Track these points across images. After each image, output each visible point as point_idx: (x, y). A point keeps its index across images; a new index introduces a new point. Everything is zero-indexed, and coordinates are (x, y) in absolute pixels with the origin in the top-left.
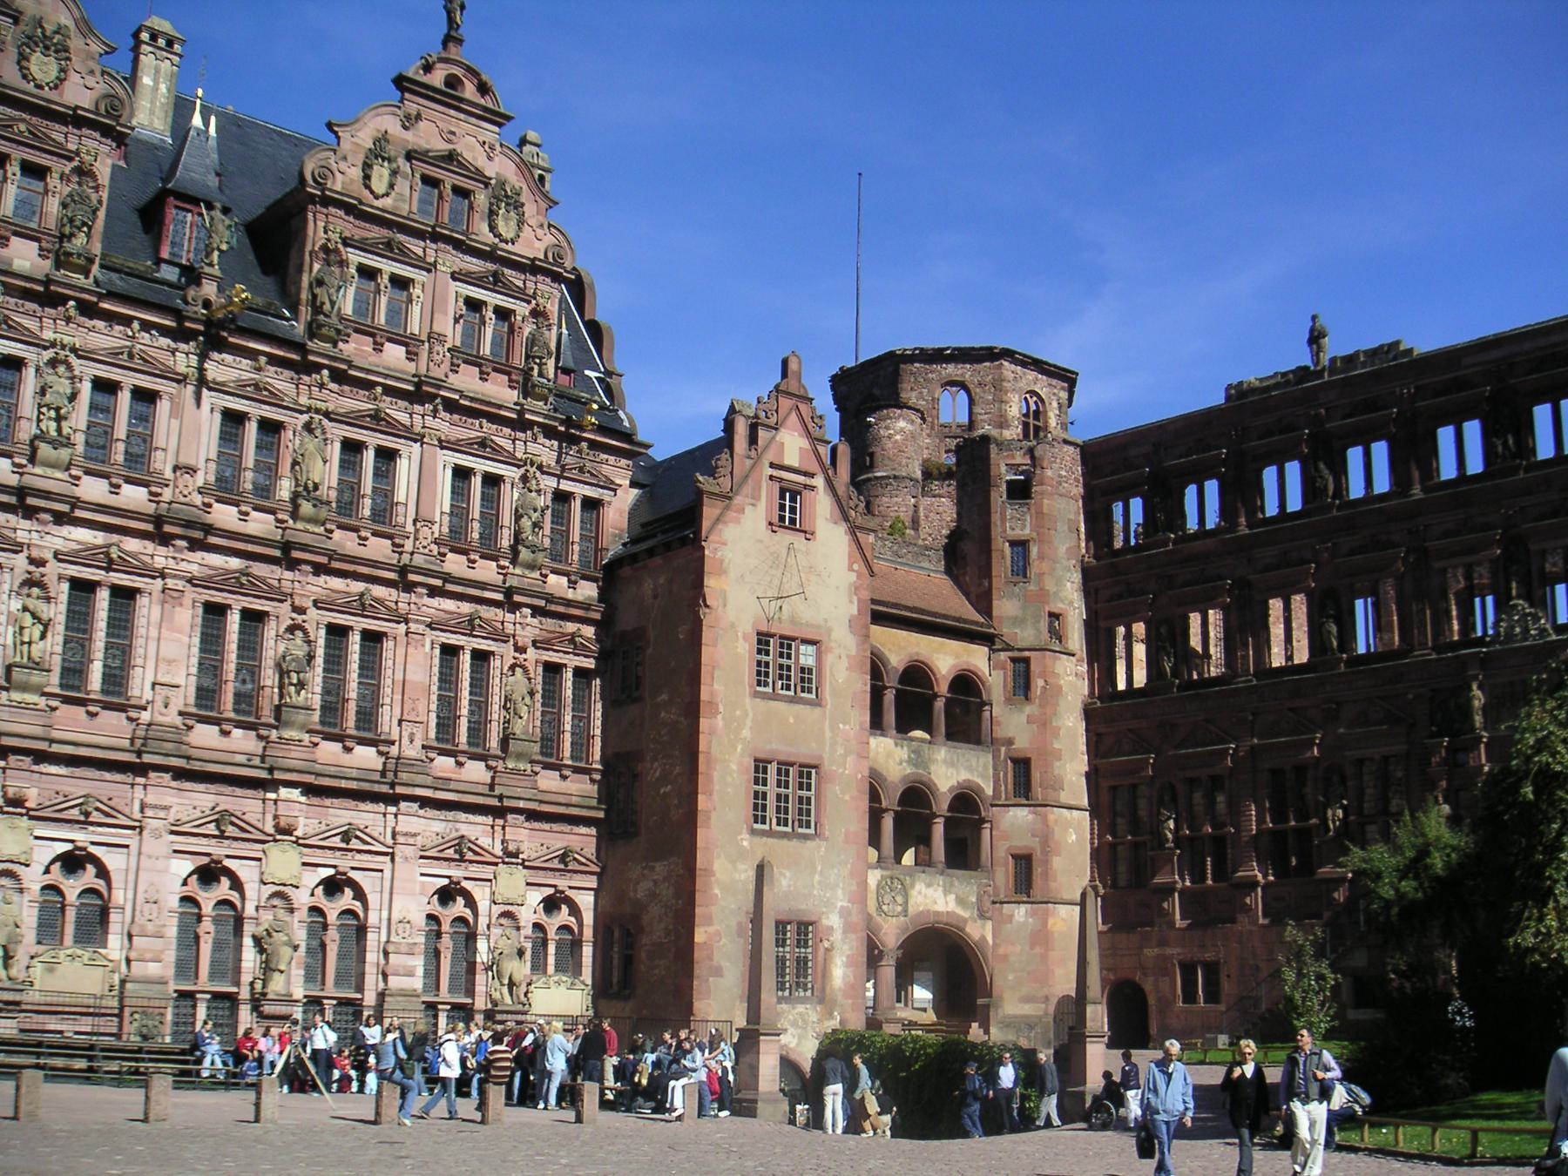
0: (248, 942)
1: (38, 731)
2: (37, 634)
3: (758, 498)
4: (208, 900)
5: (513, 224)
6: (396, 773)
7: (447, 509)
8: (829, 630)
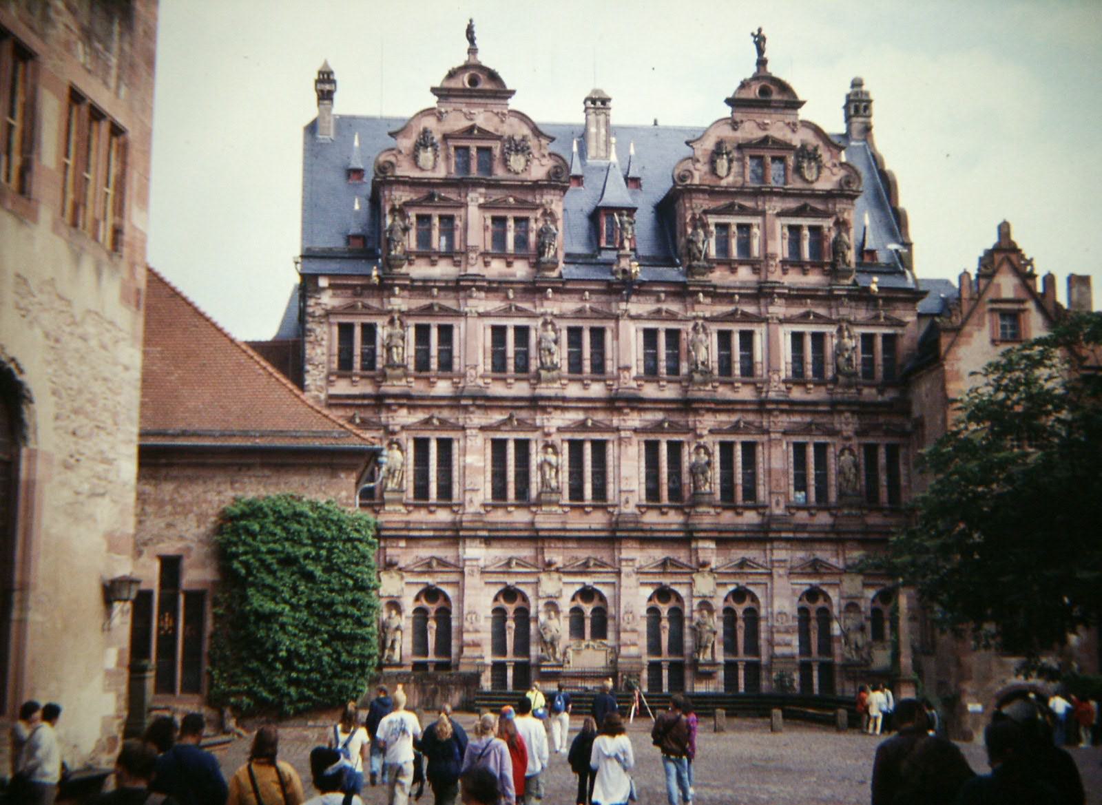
0: (687, 630)
1: (559, 526)
2: (553, 473)
4: (664, 609)
5: (815, 171)
6: (768, 524)
7: (789, 359)
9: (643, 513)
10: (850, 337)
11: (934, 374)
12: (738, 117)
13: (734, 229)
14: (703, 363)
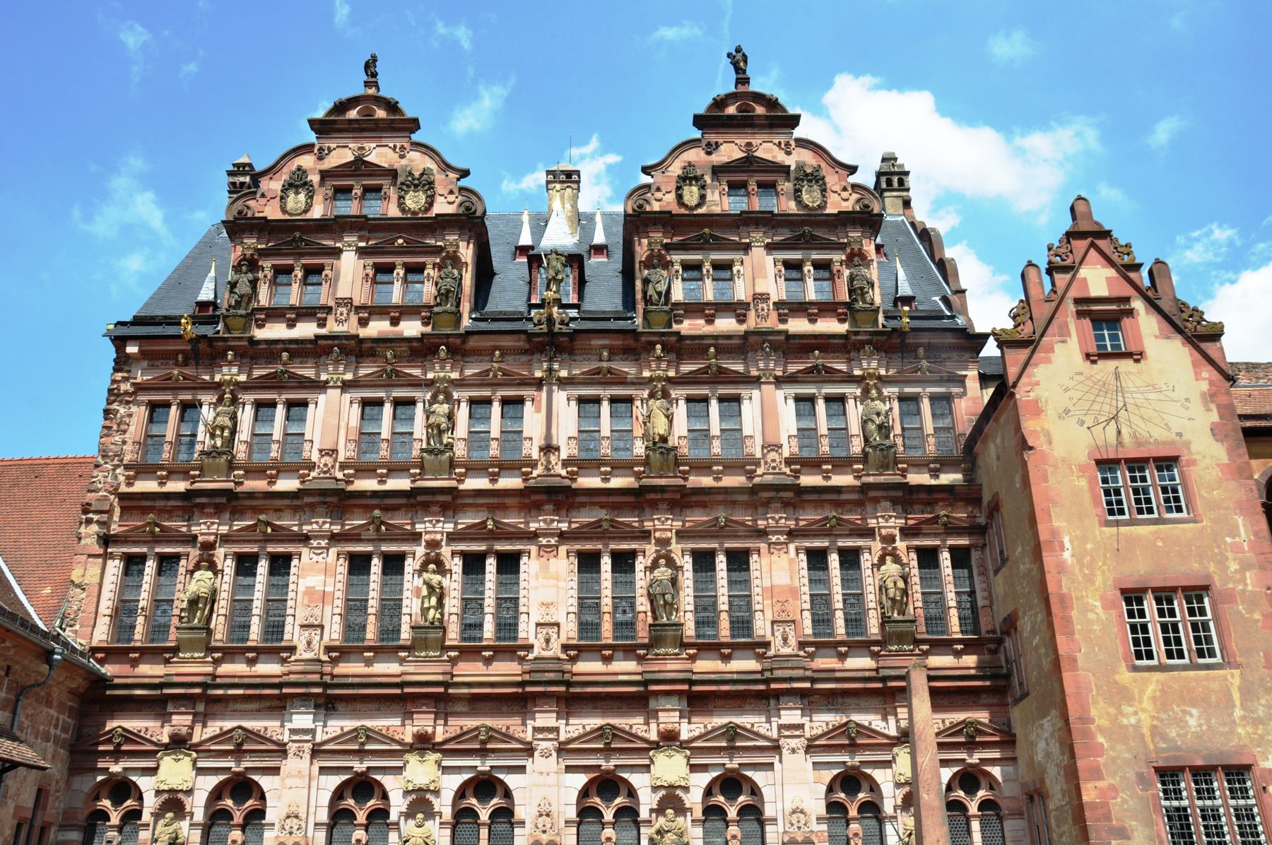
1: (440, 678)
2: (434, 600)
3: (1069, 335)
5: (817, 194)
8: (1187, 444)
9: (573, 660)
10: (882, 399)
11: (1002, 419)
12: (713, 138)
13: (707, 266)
14: (664, 439)
